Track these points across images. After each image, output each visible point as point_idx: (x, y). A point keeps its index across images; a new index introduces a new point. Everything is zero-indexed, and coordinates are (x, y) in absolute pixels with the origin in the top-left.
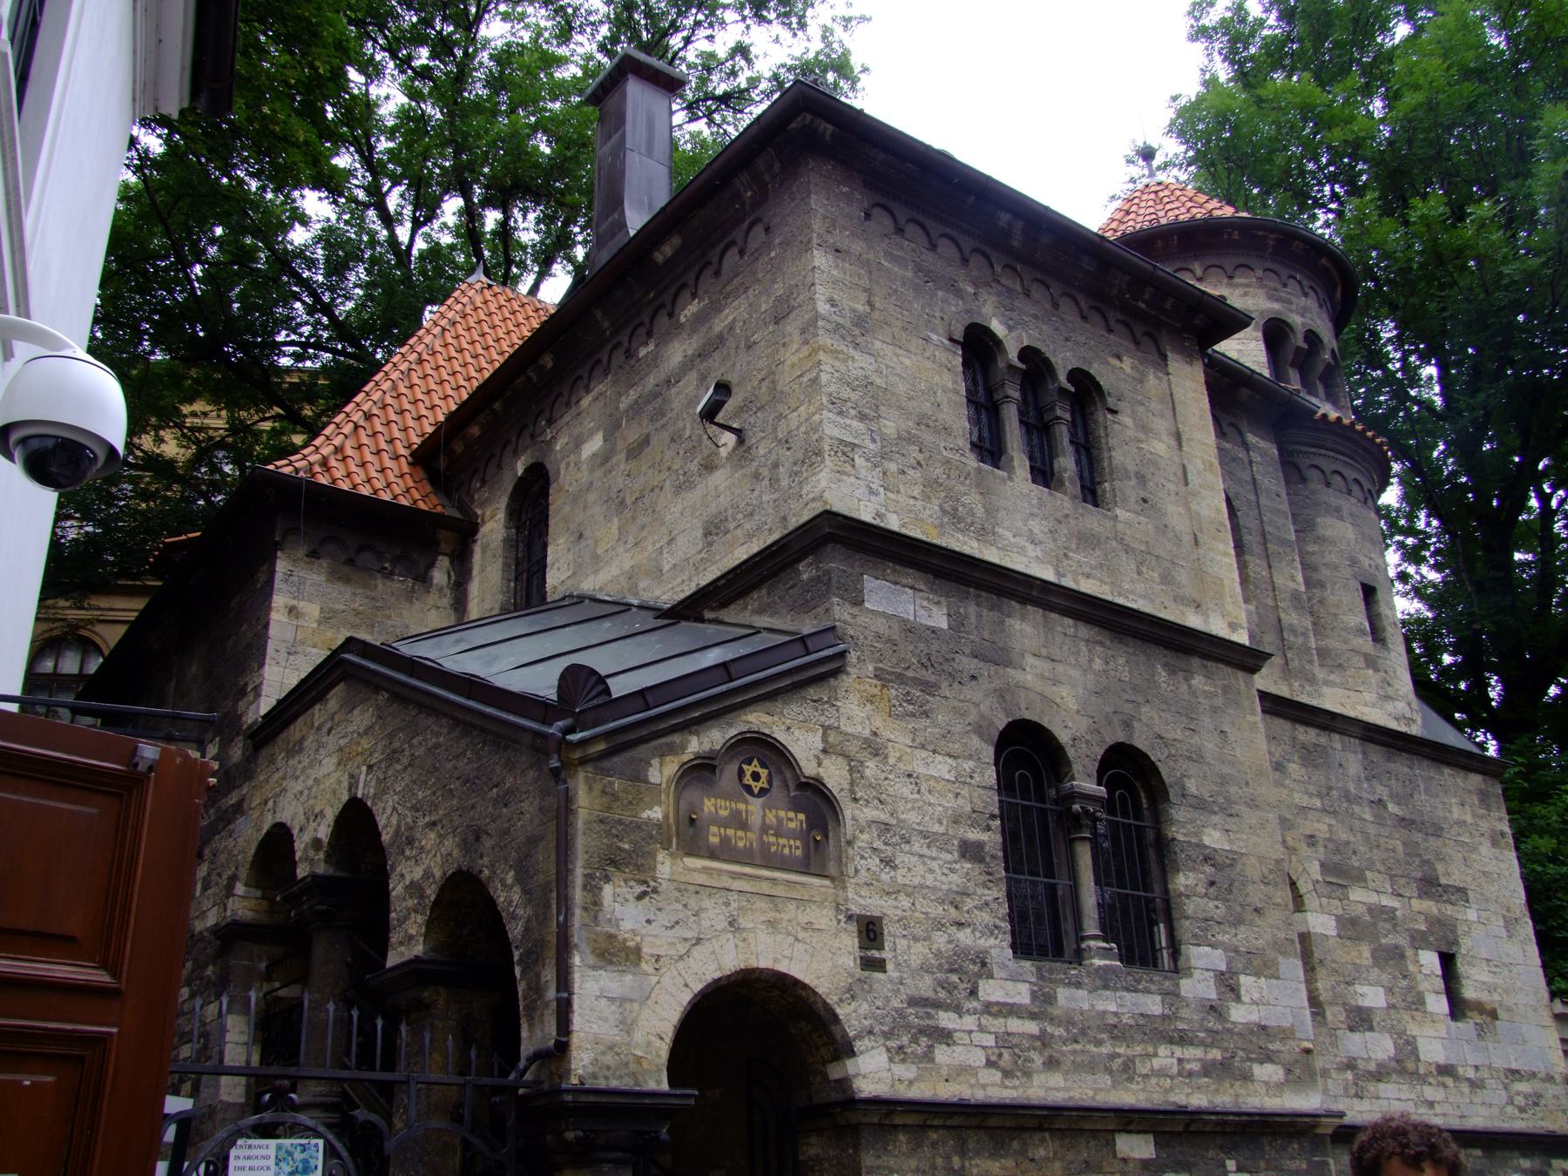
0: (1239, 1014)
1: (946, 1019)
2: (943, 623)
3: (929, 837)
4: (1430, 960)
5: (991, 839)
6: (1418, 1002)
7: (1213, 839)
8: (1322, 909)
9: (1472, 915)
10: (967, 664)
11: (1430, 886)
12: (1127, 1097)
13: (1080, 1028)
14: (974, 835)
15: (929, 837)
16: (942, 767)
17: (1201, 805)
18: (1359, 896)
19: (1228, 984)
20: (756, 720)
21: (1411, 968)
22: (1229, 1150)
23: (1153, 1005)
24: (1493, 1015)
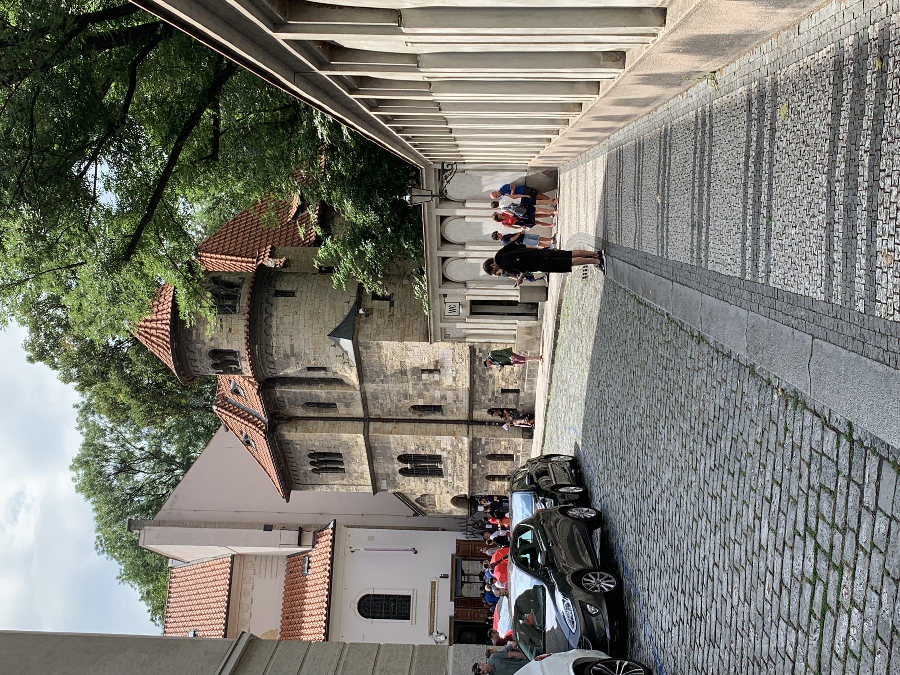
0: (449, 448)
1: (456, 486)
2: (385, 481)
3: (426, 485)
4: (425, 376)
5: (423, 480)
6: (438, 383)
7: (413, 448)
8: (417, 401)
9: (409, 361)
10: (392, 479)
11: (403, 373)
12: (467, 467)
13: (455, 471)
14: (424, 481)
15: (426, 485)
16: (413, 484)
17: (406, 448)
18: (411, 392)
19: (444, 450)
20: (413, 501)
21: (428, 382)
22: (476, 454)
23: (449, 461)
24: (437, 362)
